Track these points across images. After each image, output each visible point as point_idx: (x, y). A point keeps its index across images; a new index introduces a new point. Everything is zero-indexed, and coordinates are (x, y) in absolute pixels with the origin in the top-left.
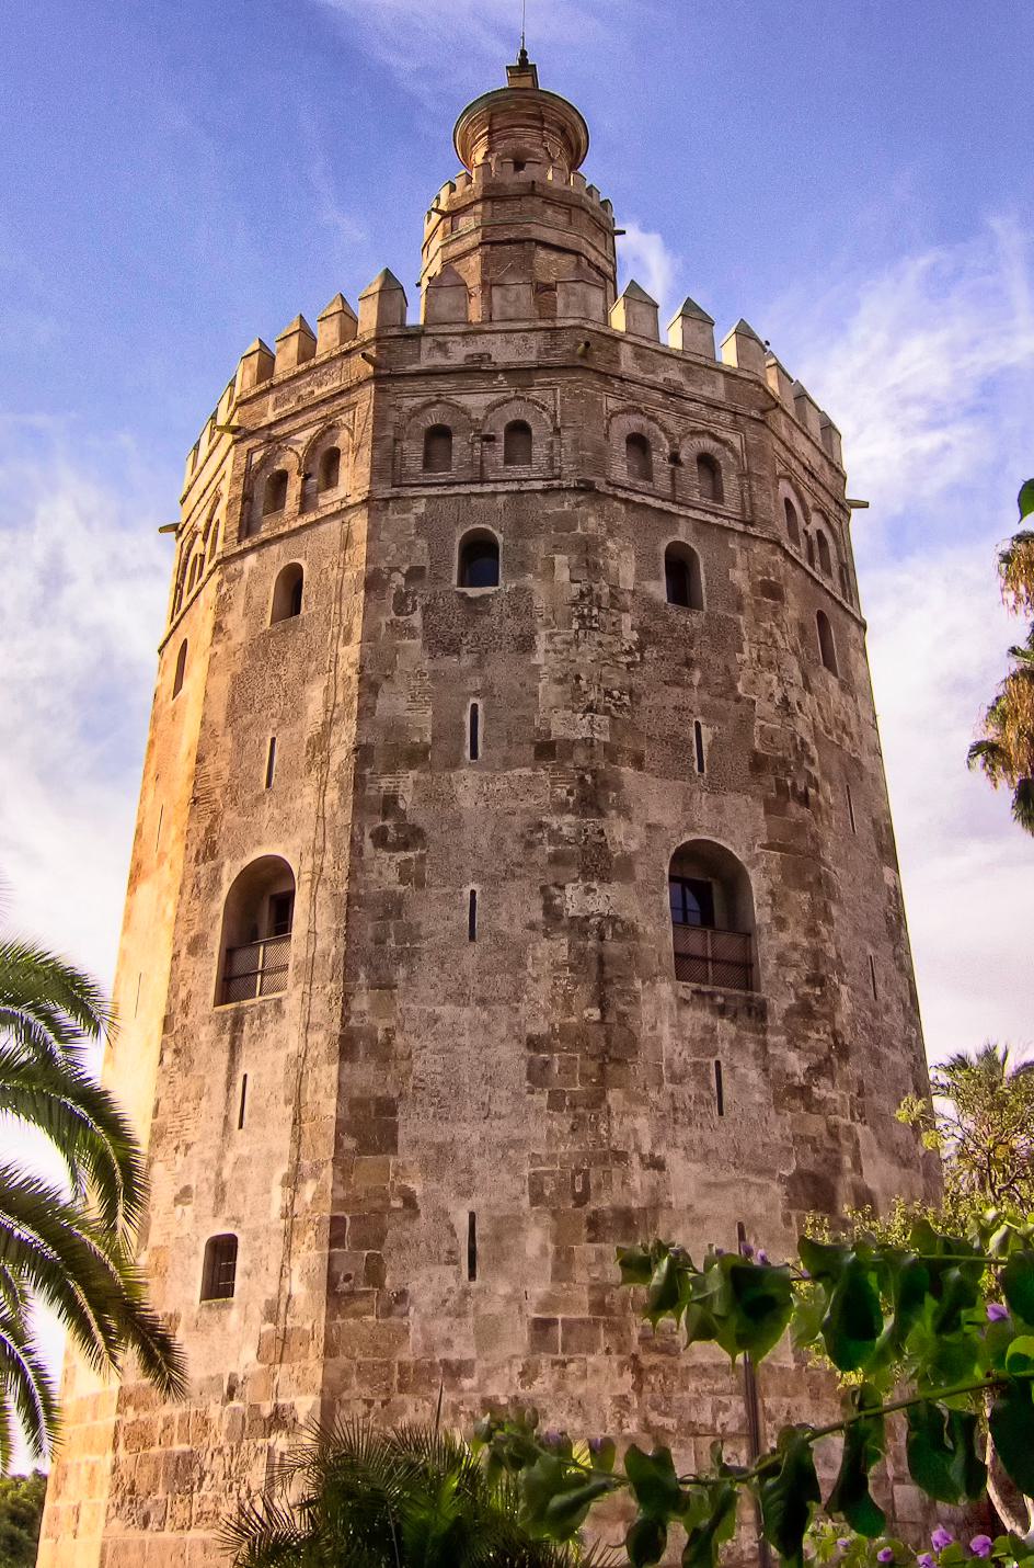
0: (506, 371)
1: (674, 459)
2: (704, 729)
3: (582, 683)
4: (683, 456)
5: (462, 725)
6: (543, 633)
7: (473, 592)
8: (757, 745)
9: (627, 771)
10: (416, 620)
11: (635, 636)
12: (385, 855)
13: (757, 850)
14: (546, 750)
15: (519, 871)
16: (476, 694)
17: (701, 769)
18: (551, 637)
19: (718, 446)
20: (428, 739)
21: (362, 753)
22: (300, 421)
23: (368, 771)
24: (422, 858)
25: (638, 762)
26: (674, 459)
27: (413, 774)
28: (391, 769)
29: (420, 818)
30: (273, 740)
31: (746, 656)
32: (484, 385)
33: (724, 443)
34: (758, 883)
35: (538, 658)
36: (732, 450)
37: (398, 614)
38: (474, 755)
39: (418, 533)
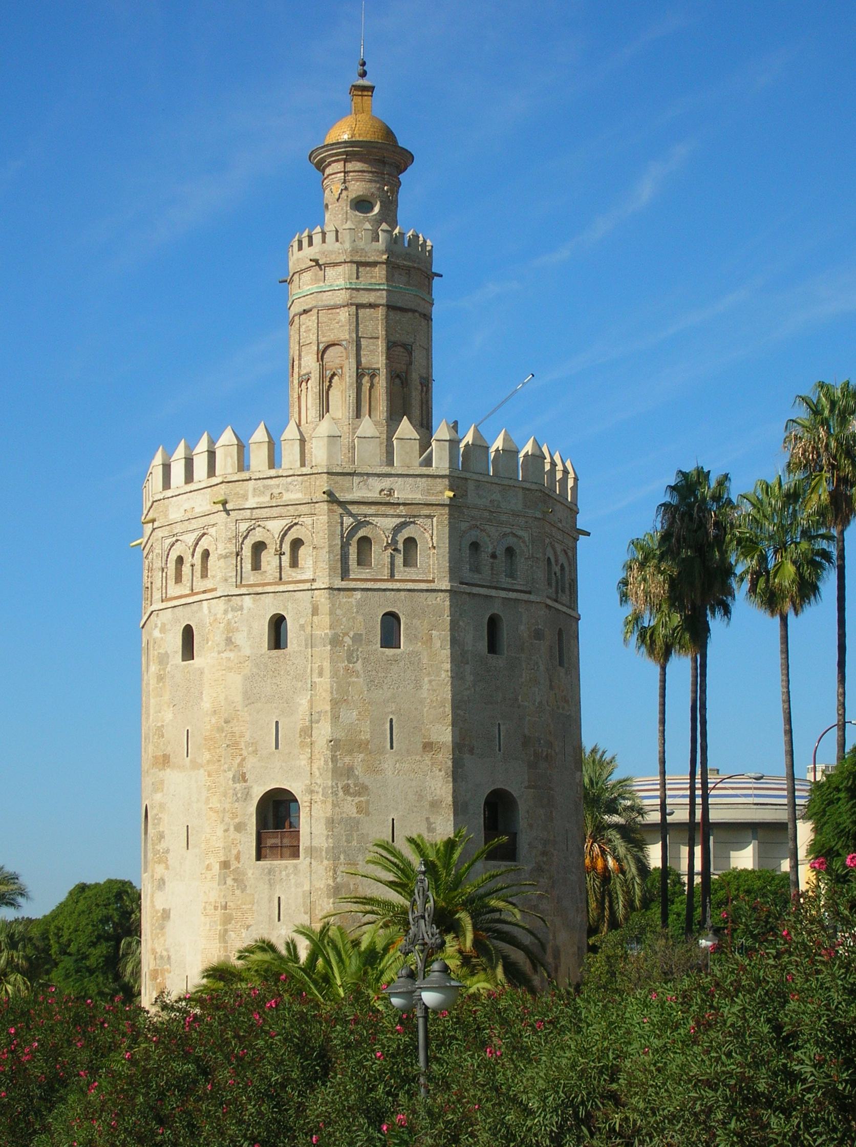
0: (404, 504)
1: (494, 556)
2: (502, 727)
3: (447, 709)
4: (498, 552)
5: (386, 730)
6: (426, 679)
7: (389, 652)
8: (526, 731)
9: (467, 756)
10: (359, 666)
11: (472, 678)
12: (349, 798)
13: (523, 789)
14: (428, 746)
15: (415, 809)
16: (392, 713)
17: (500, 750)
18: (430, 682)
19: (515, 539)
20: (368, 737)
21: (335, 744)
22: (275, 512)
23: (338, 753)
24: (367, 802)
25: (471, 751)
26: (494, 556)
27: (361, 756)
28: (350, 752)
29: (365, 779)
30: (277, 722)
31: (523, 680)
32: (391, 512)
33: (520, 538)
34: (523, 807)
35: (424, 693)
36: (524, 542)
37: (349, 662)
38: (392, 747)
39: (357, 612)
